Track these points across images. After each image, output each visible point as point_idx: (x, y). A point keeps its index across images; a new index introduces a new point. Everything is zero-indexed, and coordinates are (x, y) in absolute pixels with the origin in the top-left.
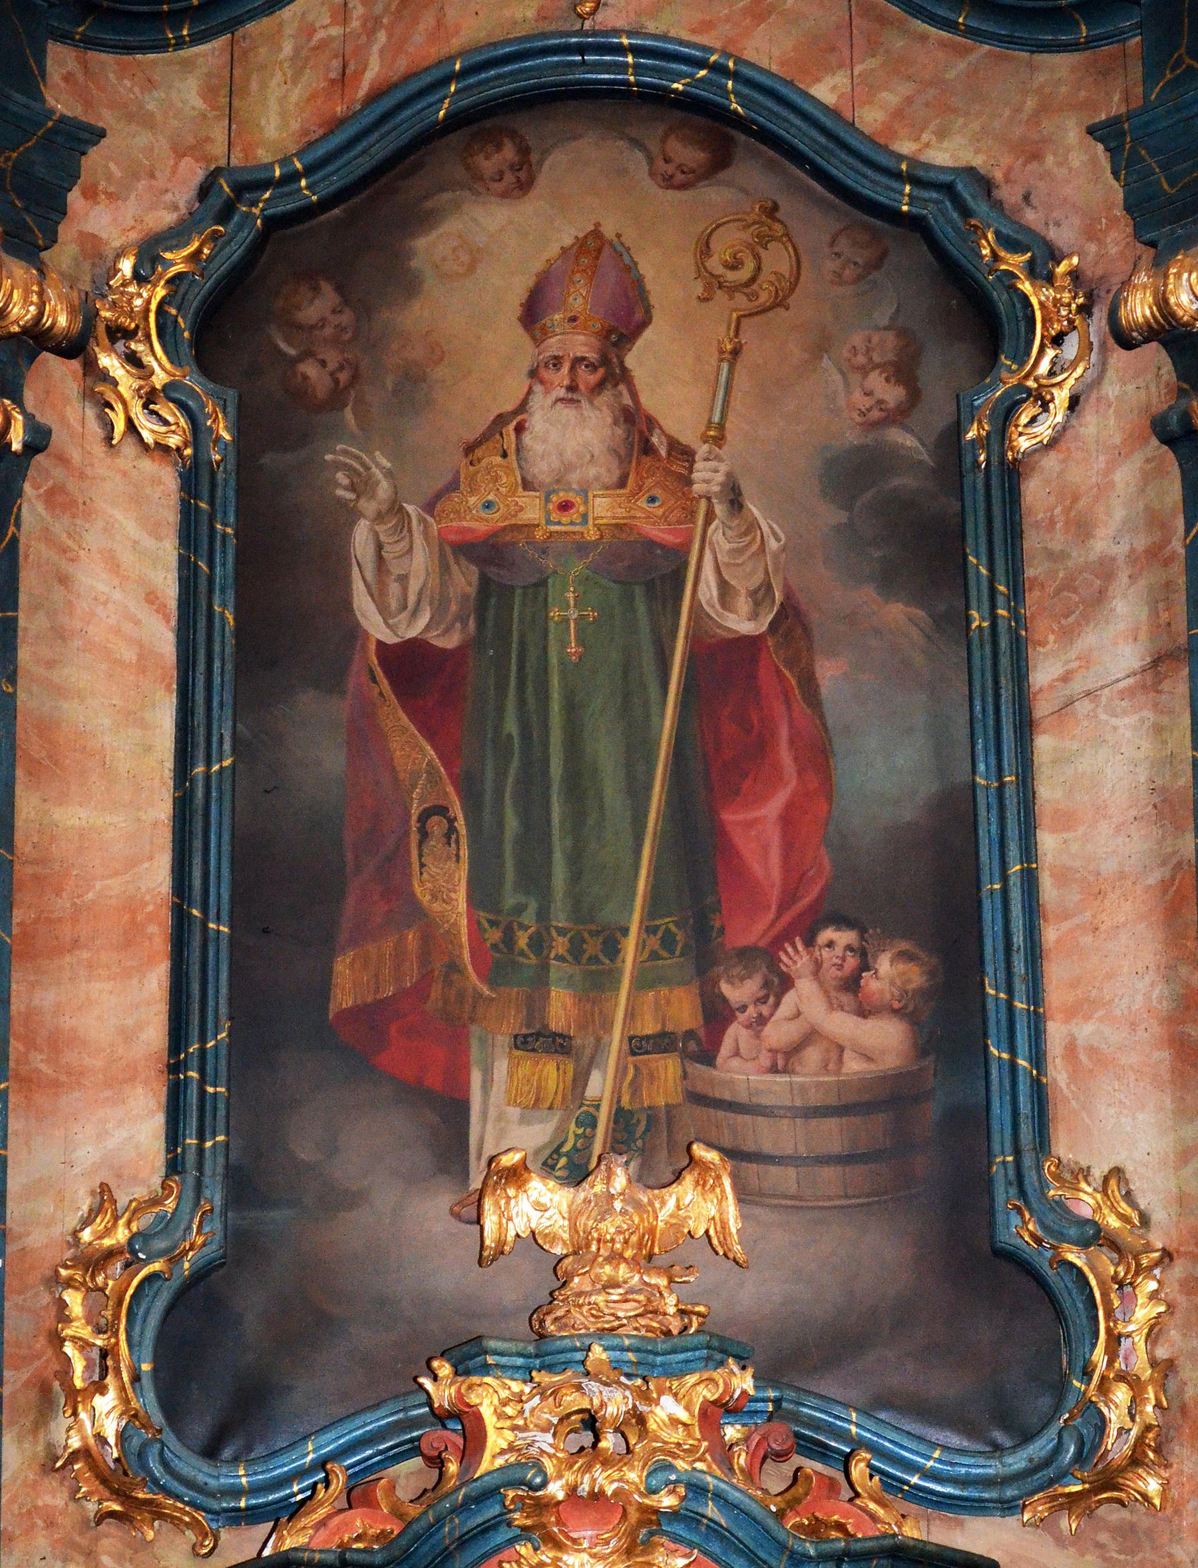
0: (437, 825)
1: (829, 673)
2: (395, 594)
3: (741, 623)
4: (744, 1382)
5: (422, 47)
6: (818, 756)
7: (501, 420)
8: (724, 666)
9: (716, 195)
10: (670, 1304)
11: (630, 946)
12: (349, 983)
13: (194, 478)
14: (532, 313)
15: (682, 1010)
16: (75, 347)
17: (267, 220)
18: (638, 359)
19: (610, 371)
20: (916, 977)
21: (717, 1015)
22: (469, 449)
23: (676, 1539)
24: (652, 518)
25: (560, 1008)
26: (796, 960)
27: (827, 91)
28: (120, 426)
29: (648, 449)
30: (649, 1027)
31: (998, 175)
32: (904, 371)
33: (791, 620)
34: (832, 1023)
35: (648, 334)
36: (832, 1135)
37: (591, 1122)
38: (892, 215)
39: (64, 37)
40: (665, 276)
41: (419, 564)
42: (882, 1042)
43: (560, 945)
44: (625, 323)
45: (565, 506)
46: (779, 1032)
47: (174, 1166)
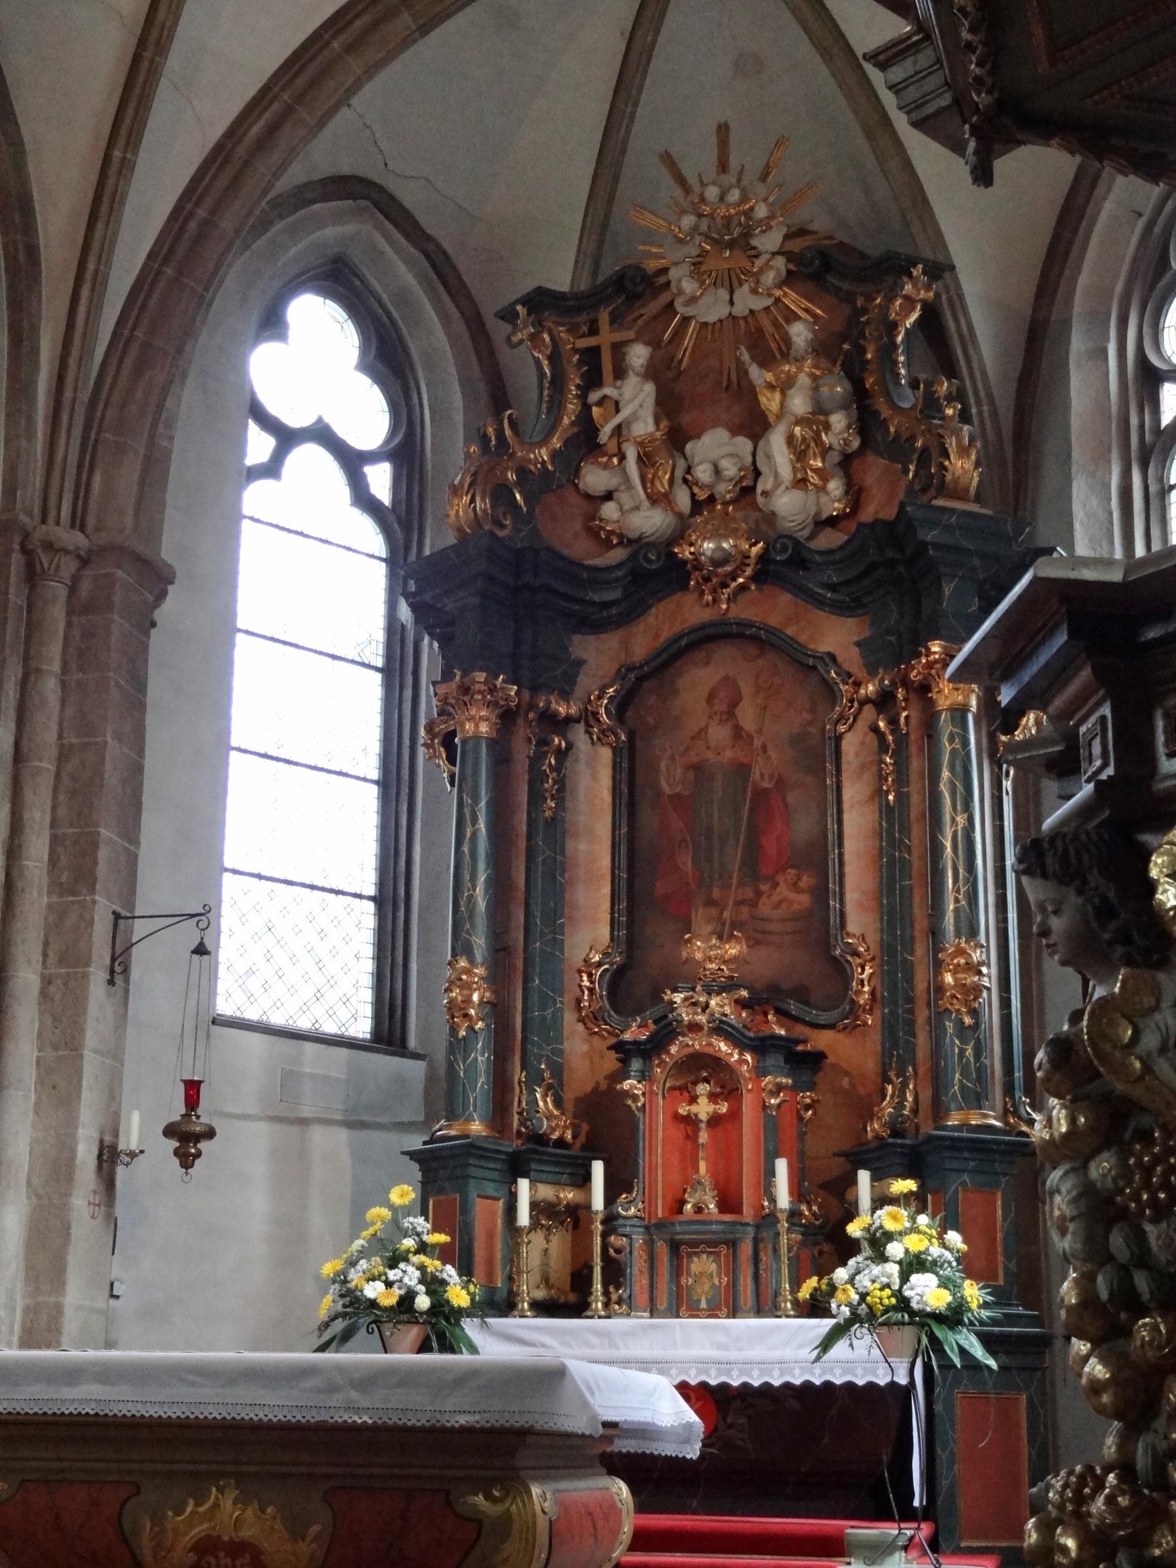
0: (683, 844)
1: (791, 797)
3: (766, 784)
4: (744, 993)
5: (678, 628)
7: (701, 730)
8: (760, 796)
9: (760, 662)
11: (735, 876)
13: (615, 750)
14: (710, 699)
15: (749, 893)
17: (637, 678)
19: (730, 714)
20: (813, 881)
21: (759, 894)
22: (692, 738)
23: (717, 1035)
25: (716, 893)
26: (781, 878)
27: (790, 631)
28: (595, 737)
29: (741, 736)
30: (740, 898)
31: (837, 654)
32: (812, 710)
33: (780, 783)
34: (788, 896)
35: (742, 703)
36: (790, 926)
37: (724, 924)
38: (808, 666)
39: (579, 633)
40: (746, 689)
41: (679, 772)
42: (804, 900)
43: (716, 876)
44: (735, 702)
45: (719, 754)
46: (775, 898)
47: (612, 939)
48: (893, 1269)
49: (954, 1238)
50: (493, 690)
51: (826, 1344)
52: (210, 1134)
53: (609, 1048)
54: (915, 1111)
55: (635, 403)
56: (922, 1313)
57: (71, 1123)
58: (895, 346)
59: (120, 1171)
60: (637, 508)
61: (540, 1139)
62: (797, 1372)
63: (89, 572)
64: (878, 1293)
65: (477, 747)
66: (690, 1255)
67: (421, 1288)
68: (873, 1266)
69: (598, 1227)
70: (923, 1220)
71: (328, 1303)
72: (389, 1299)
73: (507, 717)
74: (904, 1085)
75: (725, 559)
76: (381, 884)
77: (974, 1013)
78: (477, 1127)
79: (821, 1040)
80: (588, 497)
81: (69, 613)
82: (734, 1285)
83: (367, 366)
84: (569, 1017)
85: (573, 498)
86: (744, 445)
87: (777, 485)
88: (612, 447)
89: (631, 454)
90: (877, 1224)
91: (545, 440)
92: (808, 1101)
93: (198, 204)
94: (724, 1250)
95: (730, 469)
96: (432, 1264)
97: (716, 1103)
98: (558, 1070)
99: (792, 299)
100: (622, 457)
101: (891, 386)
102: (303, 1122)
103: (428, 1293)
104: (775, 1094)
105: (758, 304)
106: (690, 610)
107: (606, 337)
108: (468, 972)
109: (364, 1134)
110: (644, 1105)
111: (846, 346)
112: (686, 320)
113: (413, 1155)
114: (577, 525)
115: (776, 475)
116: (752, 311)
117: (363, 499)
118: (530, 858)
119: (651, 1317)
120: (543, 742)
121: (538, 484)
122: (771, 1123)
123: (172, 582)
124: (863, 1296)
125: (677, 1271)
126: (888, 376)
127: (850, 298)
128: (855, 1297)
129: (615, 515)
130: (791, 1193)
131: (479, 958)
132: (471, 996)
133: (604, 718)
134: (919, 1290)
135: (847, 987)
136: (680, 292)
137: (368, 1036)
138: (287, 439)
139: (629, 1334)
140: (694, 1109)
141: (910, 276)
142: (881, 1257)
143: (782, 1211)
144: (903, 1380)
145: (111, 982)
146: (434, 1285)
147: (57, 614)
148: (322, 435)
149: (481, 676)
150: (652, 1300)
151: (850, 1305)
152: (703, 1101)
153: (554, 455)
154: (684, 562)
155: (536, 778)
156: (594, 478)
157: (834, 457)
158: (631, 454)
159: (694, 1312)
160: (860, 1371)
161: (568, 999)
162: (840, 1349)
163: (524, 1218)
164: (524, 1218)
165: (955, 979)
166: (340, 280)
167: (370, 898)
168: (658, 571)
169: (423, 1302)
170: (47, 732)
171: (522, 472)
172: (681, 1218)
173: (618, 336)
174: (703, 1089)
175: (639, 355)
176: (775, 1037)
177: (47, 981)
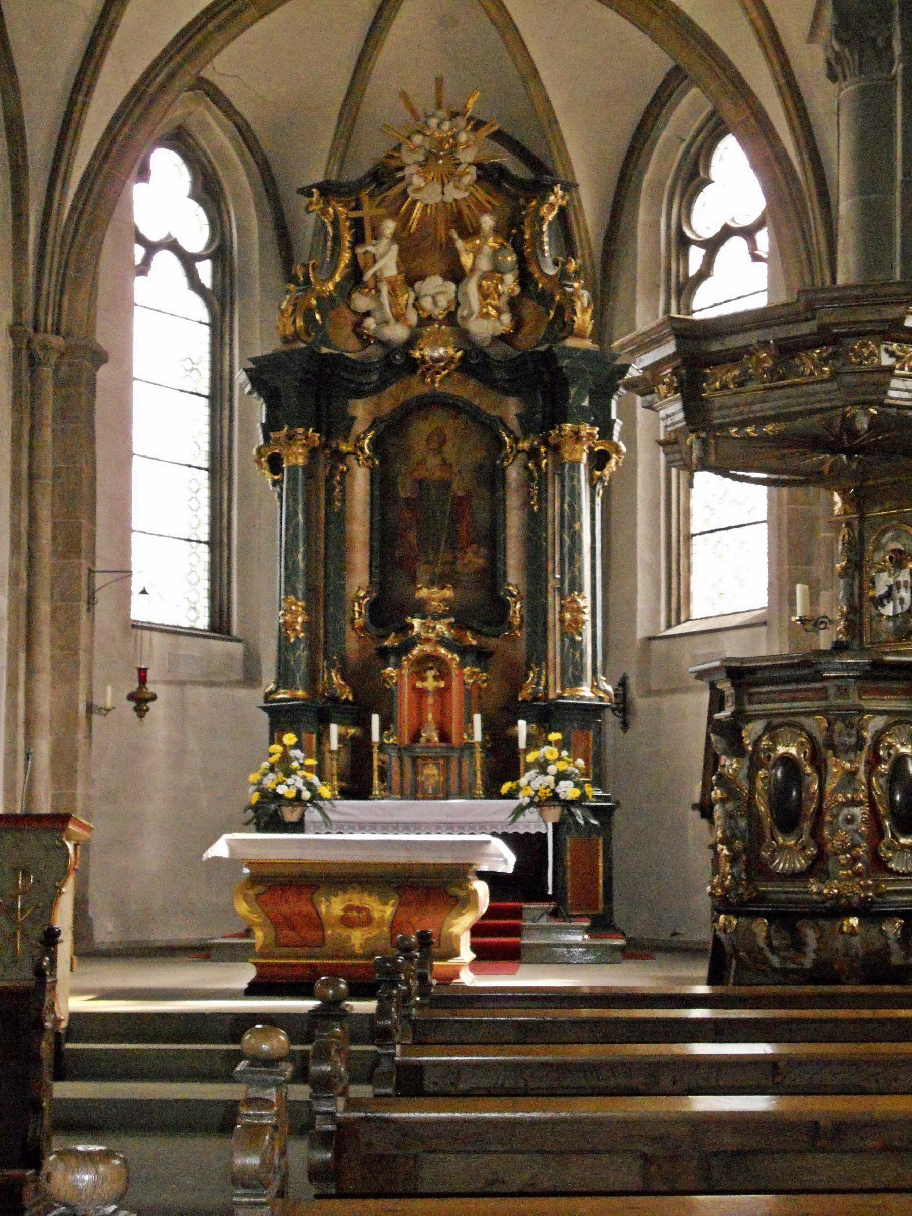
1: (475, 502)
2: (405, 490)
3: (460, 493)
4: (453, 620)
5: (409, 395)
6: (472, 515)
8: (459, 501)
12: (398, 554)
14: (428, 441)
16: (355, 454)
18: (445, 449)
19: (439, 451)
21: (455, 558)
24: (446, 476)
27: (476, 402)
34: (473, 560)
41: (408, 483)
42: (481, 562)
44: (443, 442)
46: (466, 561)
48: (550, 779)
50: (306, 438)
52: (154, 698)
54: (546, 687)
55: (388, 264)
57: (74, 692)
58: (542, 232)
59: (96, 718)
60: (386, 322)
61: (334, 699)
63: (66, 360)
65: (297, 471)
67: (304, 788)
70: (565, 753)
72: (291, 794)
73: (313, 453)
74: (540, 673)
75: (439, 360)
76: (212, 533)
77: (580, 635)
78: (301, 693)
79: (493, 643)
80: (355, 312)
81: (55, 385)
82: (447, 780)
83: (194, 195)
84: (348, 627)
85: (346, 311)
86: (452, 286)
87: (471, 314)
88: (372, 284)
89: (385, 289)
91: (331, 277)
93: (124, 124)
94: (441, 762)
95: (443, 301)
98: (343, 660)
99: (481, 195)
100: (378, 291)
101: (540, 257)
102: (182, 683)
103: (309, 790)
104: (471, 677)
105: (460, 195)
106: (417, 387)
107: (368, 211)
108: (296, 605)
111: (514, 231)
112: (415, 202)
114: (349, 330)
115: (470, 308)
116: (455, 200)
117: (195, 284)
118: (327, 536)
119: (402, 799)
120: (334, 468)
121: (327, 304)
122: (467, 693)
123: (106, 361)
124: (536, 792)
125: (416, 773)
126: (538, 251)
127: (515, 198)
128: (533, 793)
129: (373, 326)
131: (300, 596)
133: (367, 451)
135: (506, 613)
136: (410, 184)
138: (152, 248)
139: (399, 808)
140: (425, 684)
141: (553, 190)
145: (88, 610)
146: (309, 786)
147: (49, 387)
148: (173, 245)
149: (301, 430)
152: (430, 680)
153: (337, 285)
154: (416, 359)
155: (330, 490)
156: (361, 302)
157: (504, 299)
158: (385, 289)
161: (347, 617)
164: (334, 745)
166: (179, 140)
167: (205, 542)
168: (400, 362)
169: (306, 795)
170: (47, 462)
171: (318, 299)
173: (375, 212)
174: (430, 674)
175: (389, 226)
176: (472, 646)
177: (54, 610)
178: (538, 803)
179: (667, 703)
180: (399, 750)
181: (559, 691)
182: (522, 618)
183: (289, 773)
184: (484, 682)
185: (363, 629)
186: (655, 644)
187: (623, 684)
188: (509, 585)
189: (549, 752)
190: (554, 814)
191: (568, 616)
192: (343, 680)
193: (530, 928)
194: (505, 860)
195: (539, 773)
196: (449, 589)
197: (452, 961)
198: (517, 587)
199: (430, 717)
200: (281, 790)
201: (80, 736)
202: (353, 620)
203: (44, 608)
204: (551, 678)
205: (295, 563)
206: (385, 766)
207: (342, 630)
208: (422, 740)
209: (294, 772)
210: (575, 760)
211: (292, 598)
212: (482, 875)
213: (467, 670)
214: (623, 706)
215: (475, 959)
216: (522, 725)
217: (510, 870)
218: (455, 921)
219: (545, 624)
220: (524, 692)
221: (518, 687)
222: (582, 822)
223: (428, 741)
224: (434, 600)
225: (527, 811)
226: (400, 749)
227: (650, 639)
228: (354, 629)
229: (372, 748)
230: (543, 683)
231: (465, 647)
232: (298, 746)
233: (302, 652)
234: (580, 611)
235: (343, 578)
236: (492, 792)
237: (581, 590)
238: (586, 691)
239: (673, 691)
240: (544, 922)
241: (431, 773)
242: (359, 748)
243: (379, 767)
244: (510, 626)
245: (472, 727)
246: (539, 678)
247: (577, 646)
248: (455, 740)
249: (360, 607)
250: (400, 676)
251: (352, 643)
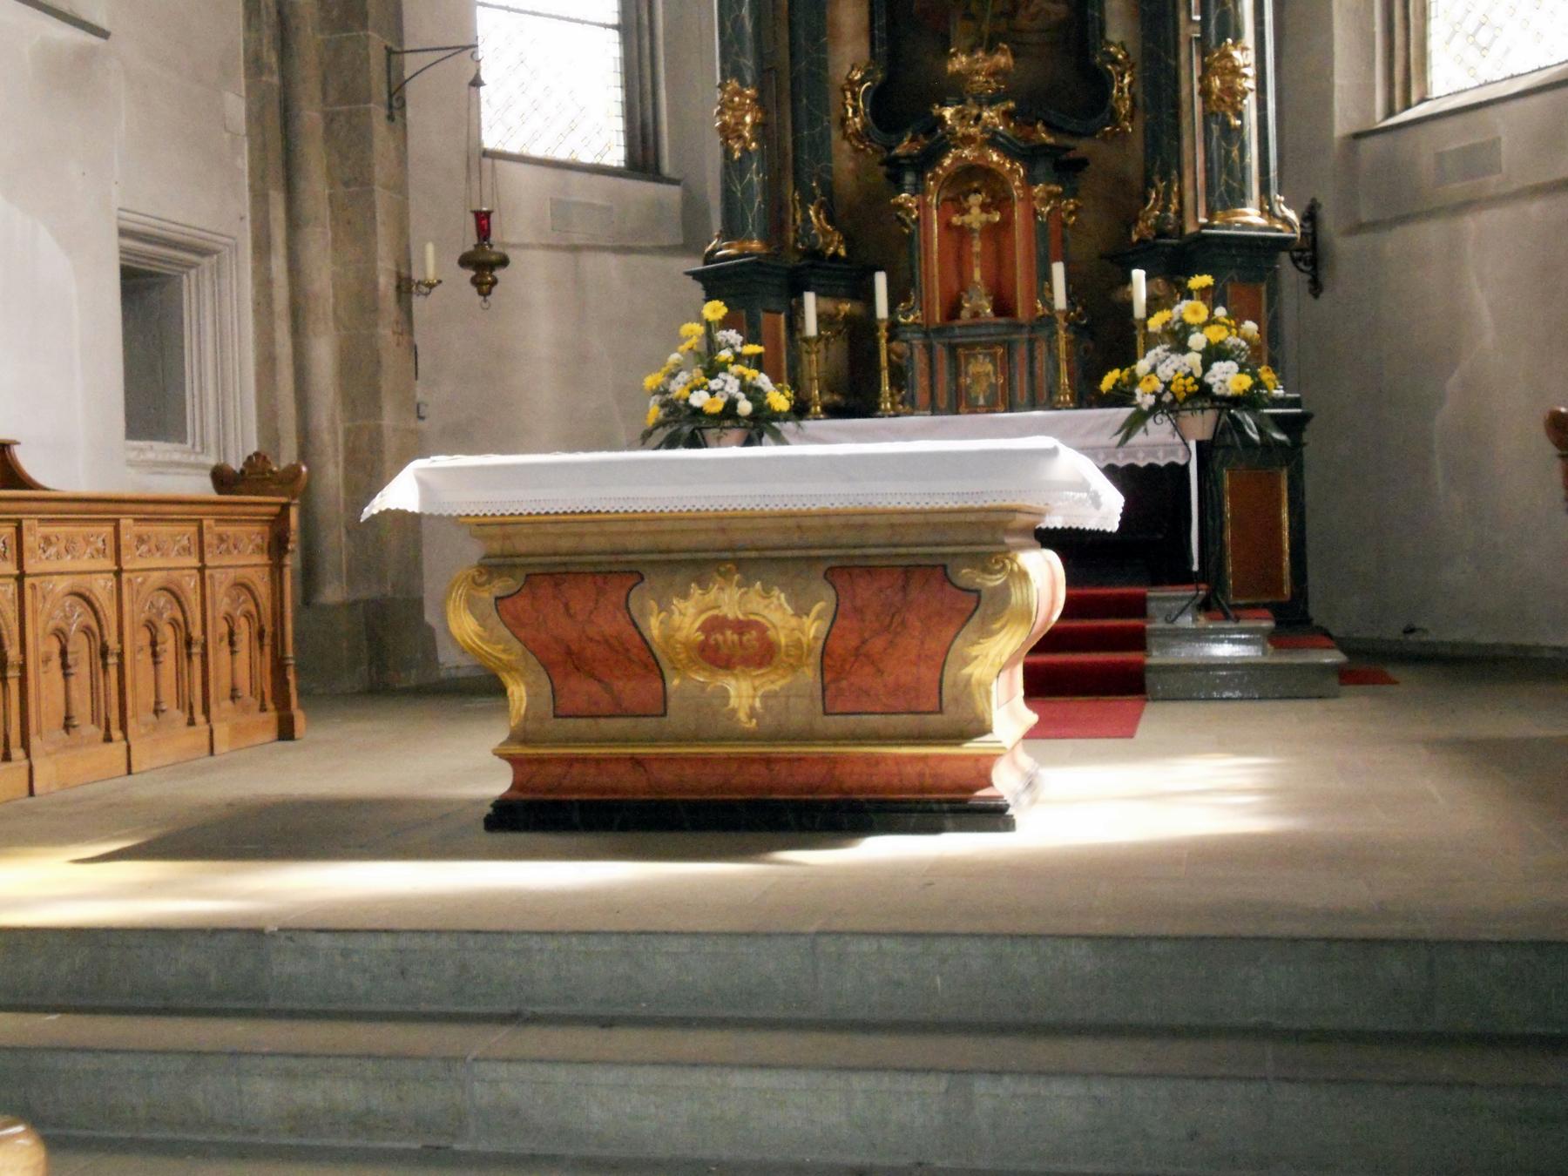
4: (1011, 105)
10: (994, 85)
48: (1194, 359)
49: (1250, 326)
51: (1130, 427)
52: (504, 262)
53: (881, 164)
56: (1223, 398)
57: (370, 257)
59: (417, 302)
61: (814, 255)
62: (1141, 455)
64: (1181, 381)
66: (967, 357)
67: (741, 396)
68: (1173, 357)
69: (883, 334)
70: (1220, 312)
71: (654, 412)
72: (716, 405)
74: (1169, 188)
77: (1240, 115)
78: (756, 245)
79: (1083, 147)
82: (1009, 381)
84: (836, 135)
90: (1176, 318)
92: (1071, 207)
94: (1000, 351)
96: (750, 374)
97: (988, 212)
98: (828, 188)
102: (575, 249)
103: (749, 398)
104: (1045, 202)
108: (740, 94)
109: (635, 259)
110: (918, 218)
113: (696, 275)
124: (1167, 385)
125: (956, 373)
128: (1160, 387)
130: (1068, 296)
131: (749, 79)
132: (743, 116)
134: (1222, 377)
135: (1106, 94)
137: (622, 164)
142: (1183, 348)
143: (1060, 311)
144: (1182, 462)
145: (391, 118)
150: (932, 397)
151: (1154, 393)
152: (976, 211)
159: (973, 409)
160: (1161, 454)
161: (834, 116)
162: (1138, 438)
163: (811, 327)
164: (811, 327)
165: (1222, 82)
169: (745, 407)
172: (958, 322)
174: (976, 200)
176: (1045, 145)
177: (330, 119)
178: (1169, 405)
179: (1393, 242)
180: (926, 334)
181: (1203, 220)
182: (1133, 99)
183: (712, 370)
184: (1071, 213)
185: (859, 136)
186: (1367, 145)
187: (1311, 216)
188: (1111, 44)
189: (1190, 310)
190: (1201, 425)
191: (1216, 83)
192: (830, 220)
193: (1162, 633)
194: (1105, 509)
195: (1171, 350)
196: (1004, 52)
197: (972, 747)
198: (1123, 46)
199: (977, 275)
200: (699, 399)
201: (386, 333)
202: (843, 120)
203: (310, 116)
204: (1188, 196)
205: (737, 21)
206: (904, 362)
207: (825, 136)
208: (965, 314)
209: (723, 368)
210: (1238, 327)
211: (733, 84)
212: (1048, 538)
213: (1038, 190)
214: (1310, 252)
215: (1037, 726)
216: (1139, 275)
217: (1112, 525)
218: (975, 651)
219: (1176, 105)
220: (1141, 225)
221: (1130, 221)
222: (1256, 437)
223: (976, 314)
224: (978, 73)
225: (1150, 422)
226: (927, 332)
227: (1358, 136)
228: (845, 137)
229: (877, 329)
230: (1173, 207)
231: (1034, 149)
232: (726, 324)
233: (755, 177)
234: (1236, 72)
235: (823, 49)
236: (1088, 396)
237: (1238, 36)
238: (1251, 215)
239: (1403, 220)
240: (1186, 621)
241: (981, 368)
242: (858, 335)
243: (889, 360)
244: (1114, 118)
245: (1051, 290)
246: (1168, 200)
247: (1233, 136)
248: (1022, 313)
249: (855, 98)
250: (923, 207)
251: (844, 160)
